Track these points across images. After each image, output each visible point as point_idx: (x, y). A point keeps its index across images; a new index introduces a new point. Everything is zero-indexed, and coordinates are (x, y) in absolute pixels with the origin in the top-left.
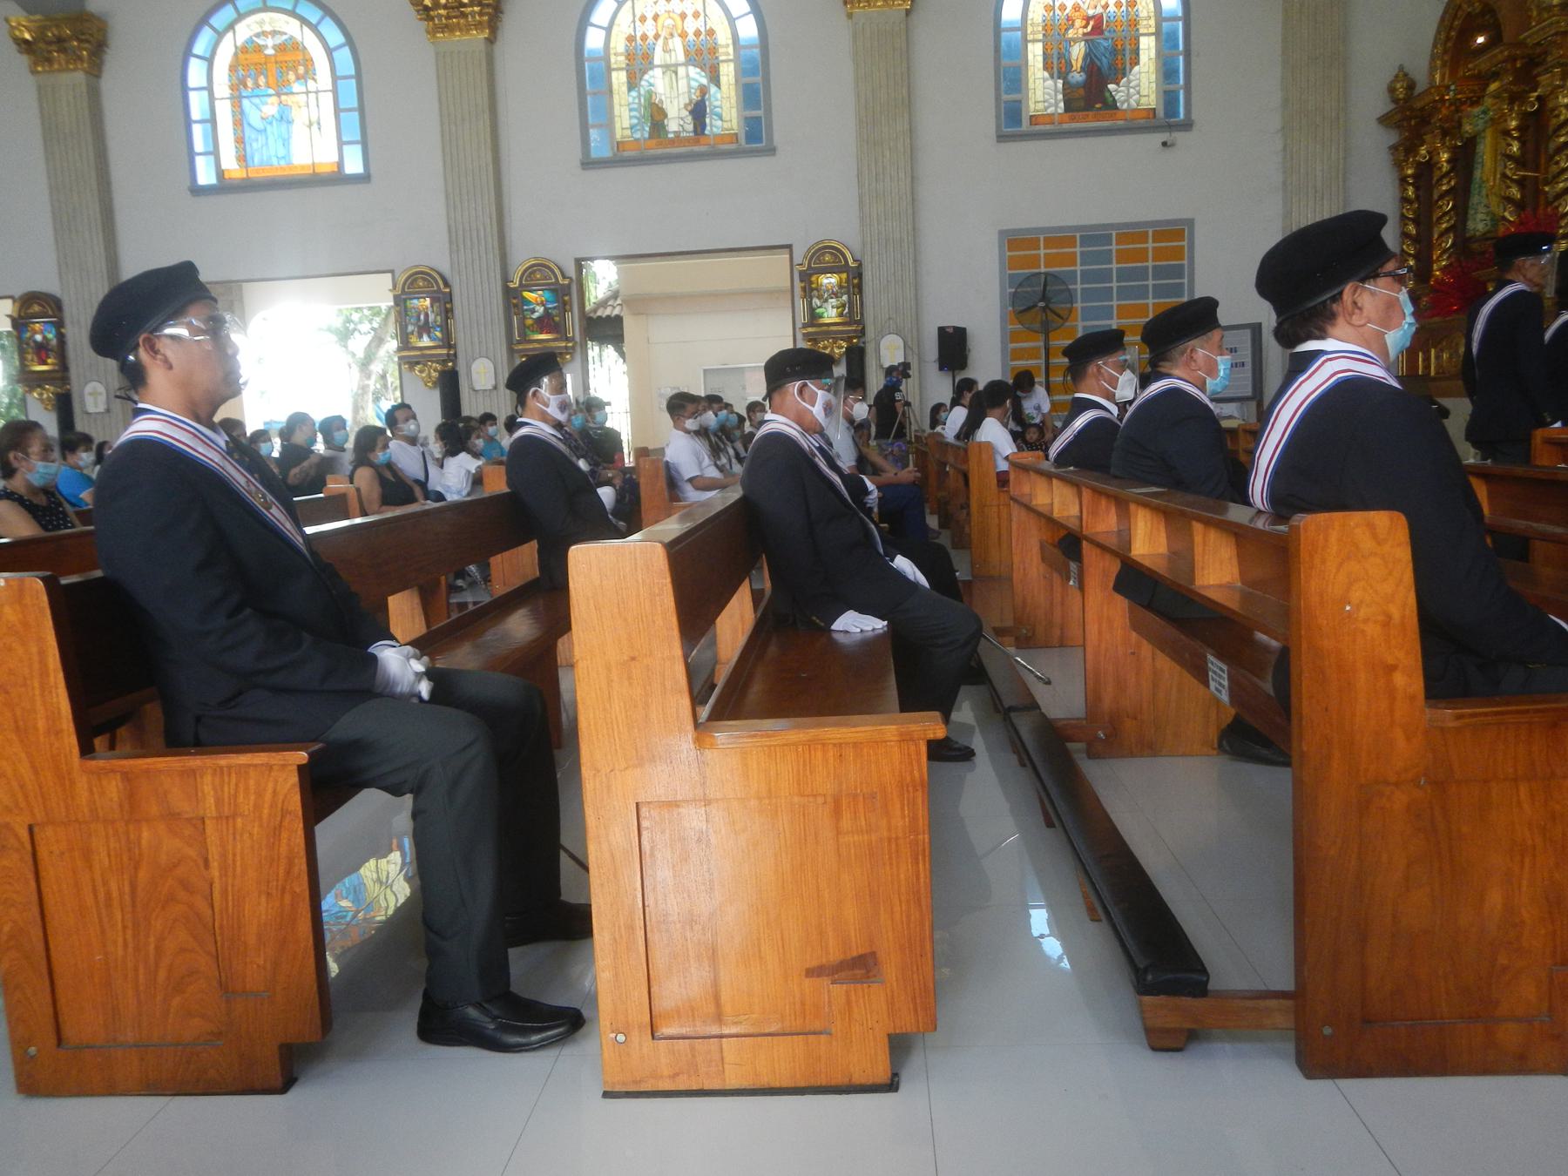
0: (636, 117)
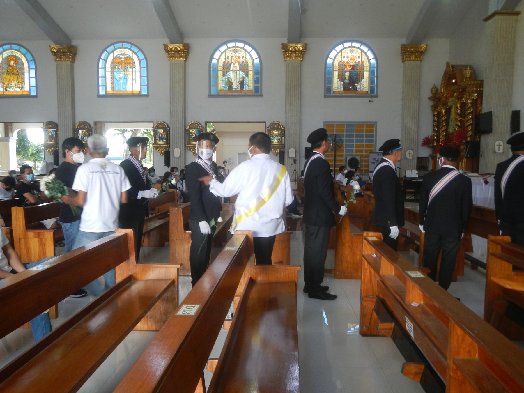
0: (224, 84)
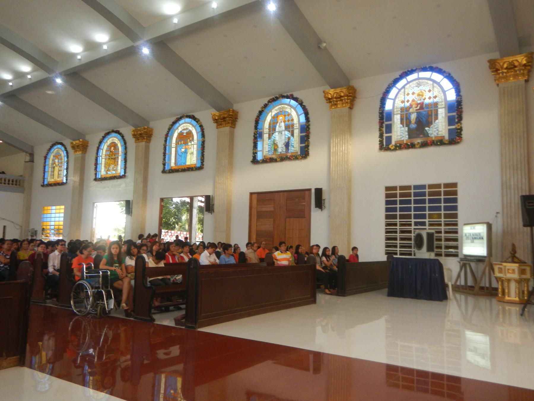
0: (270, 148)
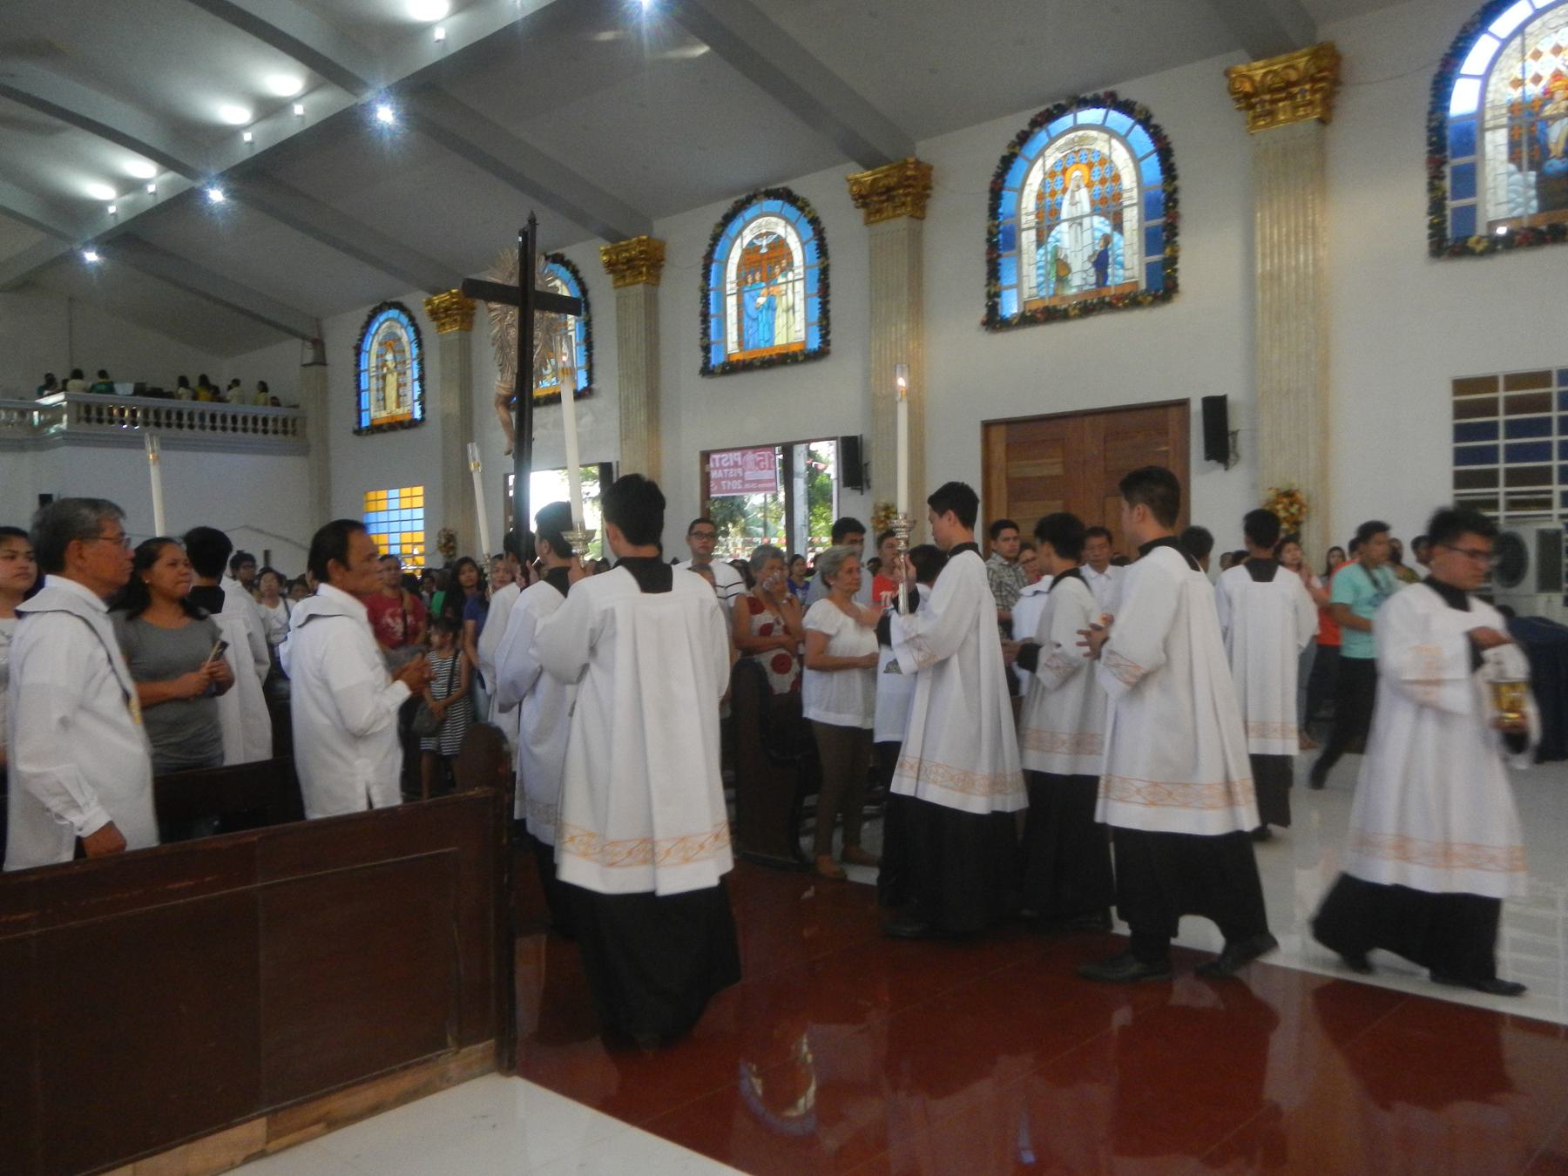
0: (1041, 275)
